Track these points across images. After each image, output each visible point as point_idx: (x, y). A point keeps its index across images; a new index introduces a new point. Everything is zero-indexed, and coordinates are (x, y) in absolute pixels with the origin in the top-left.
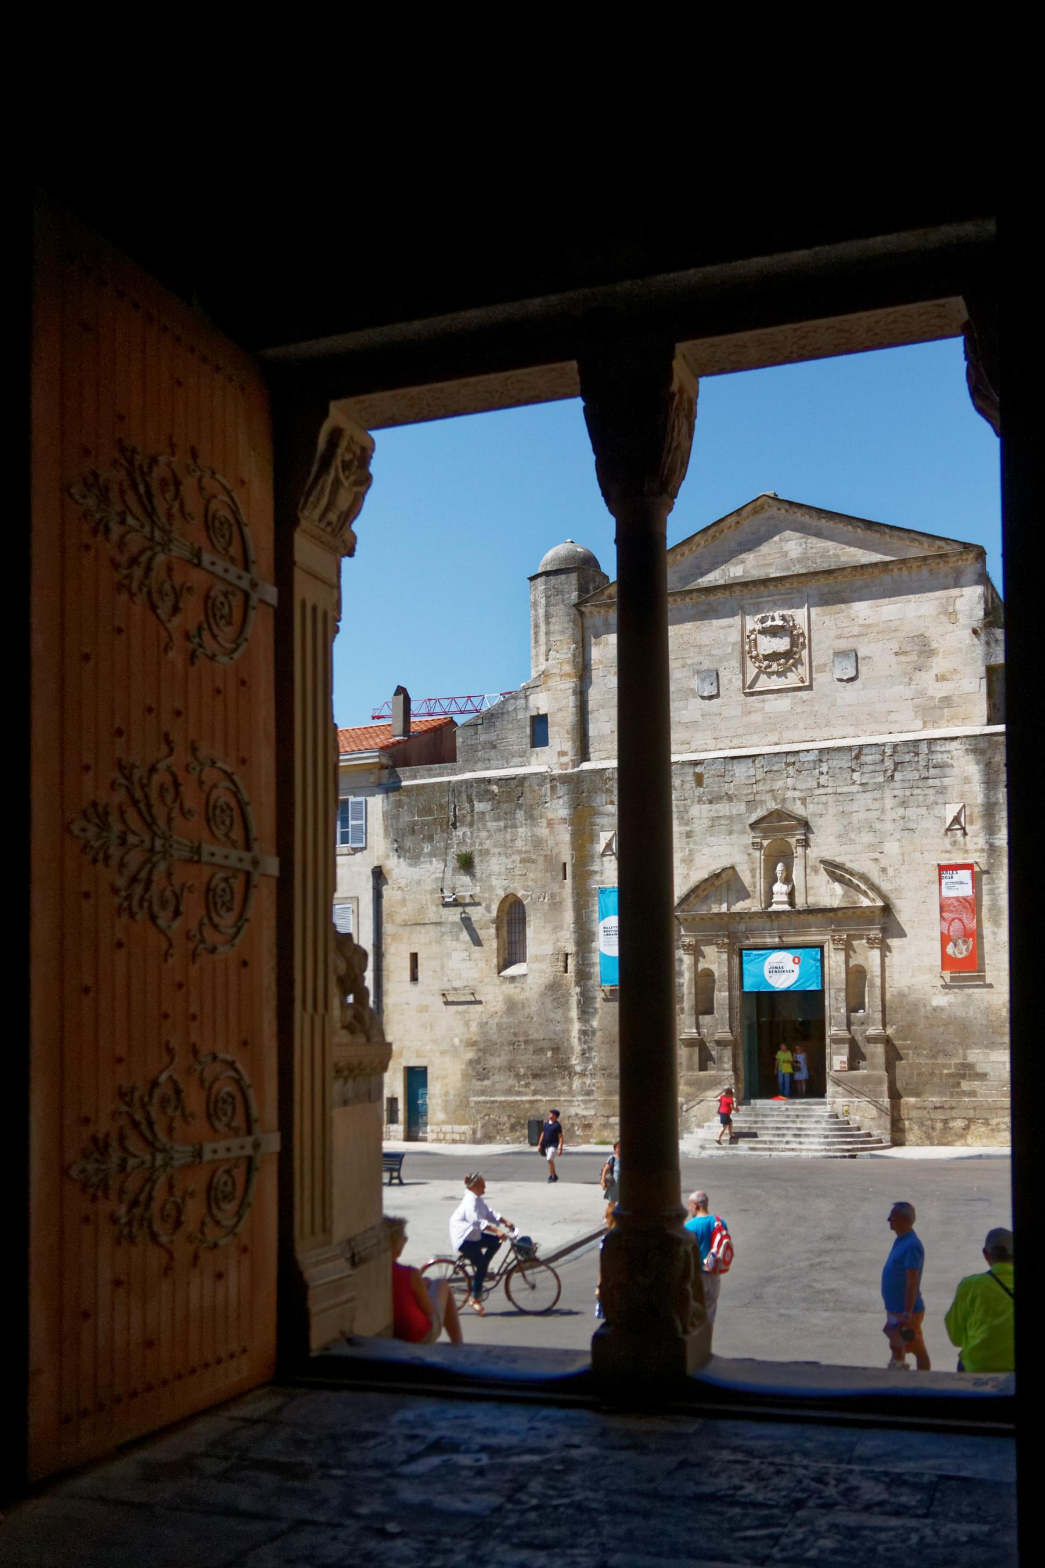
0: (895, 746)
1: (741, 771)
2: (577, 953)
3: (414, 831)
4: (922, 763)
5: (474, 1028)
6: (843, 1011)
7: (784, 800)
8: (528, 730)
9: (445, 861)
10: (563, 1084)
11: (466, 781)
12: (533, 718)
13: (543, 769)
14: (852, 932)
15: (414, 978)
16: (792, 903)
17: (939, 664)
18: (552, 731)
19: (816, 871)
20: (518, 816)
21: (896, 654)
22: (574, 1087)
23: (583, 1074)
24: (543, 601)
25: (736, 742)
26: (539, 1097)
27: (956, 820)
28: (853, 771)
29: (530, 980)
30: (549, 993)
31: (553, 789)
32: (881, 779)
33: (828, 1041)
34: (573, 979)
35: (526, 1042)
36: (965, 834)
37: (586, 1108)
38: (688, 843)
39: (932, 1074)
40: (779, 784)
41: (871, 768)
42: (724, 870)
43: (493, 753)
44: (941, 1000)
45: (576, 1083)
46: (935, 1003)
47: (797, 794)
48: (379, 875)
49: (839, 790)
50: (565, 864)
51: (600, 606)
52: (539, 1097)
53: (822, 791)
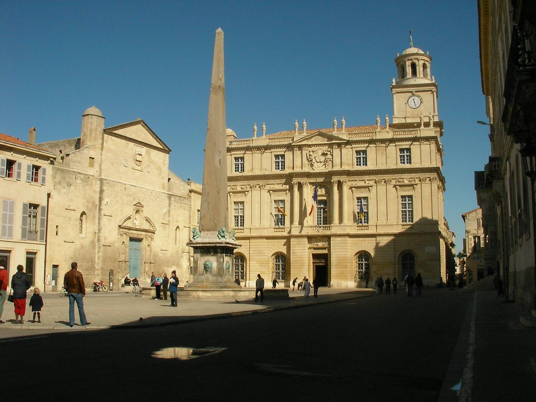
43: (79, 165)
44: (160, 255)
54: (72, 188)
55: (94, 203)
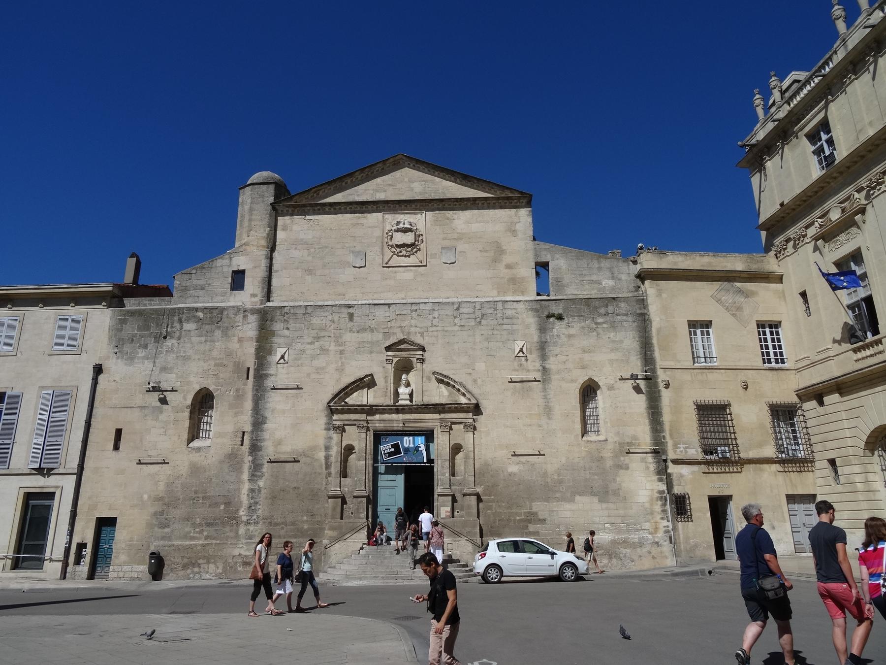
0: (482, 303)
1: (381, 313)
2: (252, 432)
3: (133, 340)
4: (499, 315)
5: (162, 486)
6: (447, 475)
7: (409, 333)
8: (230, 280)
9: (154, 362)
10: (231, 531)
11: (179, 309)
12: (234, 272)
13: (239, 304)
14: (454, 421)
15: (116, 447)
16: (411, 401)
17: (507, 259)
18: (248, 281)
19: (429, 379)
20: (216, 334)
21: (481, 251)
22: (240, 532)
23: (248, 523)
24: (249, 201)
25: (376, 296)
26: (210, 541)
27: (521, 350)
28: (455, 317)
29: (212, 450)
30: (227, 460)
31: (245, 317)
32: (473, 324)
33: (436, 496)
34: (247, 450)
35: (204, 498)
36: (527, 360)
37: (248, 549)
38: (341, 358)
39: (509, 520)
40: (406, 323)
41: (467, 316)
42: (366, 376)
43: (201, 293)
44: (513, 469)
45: (242, 530)
46: (510, 470)
47: (418, 330)
48: (98, 370)
49: (446, 329)
50: (249, 369)
51: (288, 206)
52: (210, 541)
53: (434, 329)
54: (169, 343)
55: (238, 366)
